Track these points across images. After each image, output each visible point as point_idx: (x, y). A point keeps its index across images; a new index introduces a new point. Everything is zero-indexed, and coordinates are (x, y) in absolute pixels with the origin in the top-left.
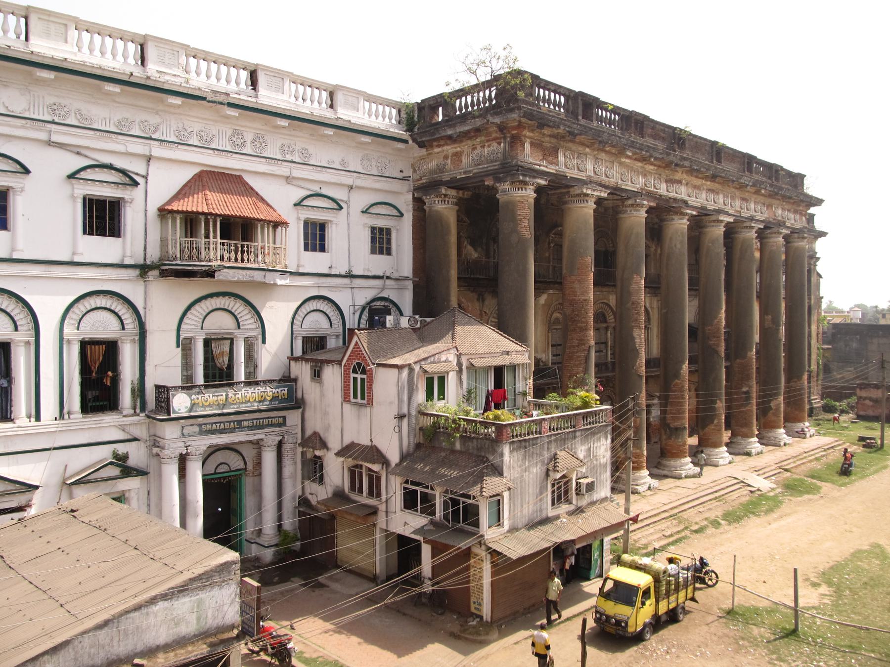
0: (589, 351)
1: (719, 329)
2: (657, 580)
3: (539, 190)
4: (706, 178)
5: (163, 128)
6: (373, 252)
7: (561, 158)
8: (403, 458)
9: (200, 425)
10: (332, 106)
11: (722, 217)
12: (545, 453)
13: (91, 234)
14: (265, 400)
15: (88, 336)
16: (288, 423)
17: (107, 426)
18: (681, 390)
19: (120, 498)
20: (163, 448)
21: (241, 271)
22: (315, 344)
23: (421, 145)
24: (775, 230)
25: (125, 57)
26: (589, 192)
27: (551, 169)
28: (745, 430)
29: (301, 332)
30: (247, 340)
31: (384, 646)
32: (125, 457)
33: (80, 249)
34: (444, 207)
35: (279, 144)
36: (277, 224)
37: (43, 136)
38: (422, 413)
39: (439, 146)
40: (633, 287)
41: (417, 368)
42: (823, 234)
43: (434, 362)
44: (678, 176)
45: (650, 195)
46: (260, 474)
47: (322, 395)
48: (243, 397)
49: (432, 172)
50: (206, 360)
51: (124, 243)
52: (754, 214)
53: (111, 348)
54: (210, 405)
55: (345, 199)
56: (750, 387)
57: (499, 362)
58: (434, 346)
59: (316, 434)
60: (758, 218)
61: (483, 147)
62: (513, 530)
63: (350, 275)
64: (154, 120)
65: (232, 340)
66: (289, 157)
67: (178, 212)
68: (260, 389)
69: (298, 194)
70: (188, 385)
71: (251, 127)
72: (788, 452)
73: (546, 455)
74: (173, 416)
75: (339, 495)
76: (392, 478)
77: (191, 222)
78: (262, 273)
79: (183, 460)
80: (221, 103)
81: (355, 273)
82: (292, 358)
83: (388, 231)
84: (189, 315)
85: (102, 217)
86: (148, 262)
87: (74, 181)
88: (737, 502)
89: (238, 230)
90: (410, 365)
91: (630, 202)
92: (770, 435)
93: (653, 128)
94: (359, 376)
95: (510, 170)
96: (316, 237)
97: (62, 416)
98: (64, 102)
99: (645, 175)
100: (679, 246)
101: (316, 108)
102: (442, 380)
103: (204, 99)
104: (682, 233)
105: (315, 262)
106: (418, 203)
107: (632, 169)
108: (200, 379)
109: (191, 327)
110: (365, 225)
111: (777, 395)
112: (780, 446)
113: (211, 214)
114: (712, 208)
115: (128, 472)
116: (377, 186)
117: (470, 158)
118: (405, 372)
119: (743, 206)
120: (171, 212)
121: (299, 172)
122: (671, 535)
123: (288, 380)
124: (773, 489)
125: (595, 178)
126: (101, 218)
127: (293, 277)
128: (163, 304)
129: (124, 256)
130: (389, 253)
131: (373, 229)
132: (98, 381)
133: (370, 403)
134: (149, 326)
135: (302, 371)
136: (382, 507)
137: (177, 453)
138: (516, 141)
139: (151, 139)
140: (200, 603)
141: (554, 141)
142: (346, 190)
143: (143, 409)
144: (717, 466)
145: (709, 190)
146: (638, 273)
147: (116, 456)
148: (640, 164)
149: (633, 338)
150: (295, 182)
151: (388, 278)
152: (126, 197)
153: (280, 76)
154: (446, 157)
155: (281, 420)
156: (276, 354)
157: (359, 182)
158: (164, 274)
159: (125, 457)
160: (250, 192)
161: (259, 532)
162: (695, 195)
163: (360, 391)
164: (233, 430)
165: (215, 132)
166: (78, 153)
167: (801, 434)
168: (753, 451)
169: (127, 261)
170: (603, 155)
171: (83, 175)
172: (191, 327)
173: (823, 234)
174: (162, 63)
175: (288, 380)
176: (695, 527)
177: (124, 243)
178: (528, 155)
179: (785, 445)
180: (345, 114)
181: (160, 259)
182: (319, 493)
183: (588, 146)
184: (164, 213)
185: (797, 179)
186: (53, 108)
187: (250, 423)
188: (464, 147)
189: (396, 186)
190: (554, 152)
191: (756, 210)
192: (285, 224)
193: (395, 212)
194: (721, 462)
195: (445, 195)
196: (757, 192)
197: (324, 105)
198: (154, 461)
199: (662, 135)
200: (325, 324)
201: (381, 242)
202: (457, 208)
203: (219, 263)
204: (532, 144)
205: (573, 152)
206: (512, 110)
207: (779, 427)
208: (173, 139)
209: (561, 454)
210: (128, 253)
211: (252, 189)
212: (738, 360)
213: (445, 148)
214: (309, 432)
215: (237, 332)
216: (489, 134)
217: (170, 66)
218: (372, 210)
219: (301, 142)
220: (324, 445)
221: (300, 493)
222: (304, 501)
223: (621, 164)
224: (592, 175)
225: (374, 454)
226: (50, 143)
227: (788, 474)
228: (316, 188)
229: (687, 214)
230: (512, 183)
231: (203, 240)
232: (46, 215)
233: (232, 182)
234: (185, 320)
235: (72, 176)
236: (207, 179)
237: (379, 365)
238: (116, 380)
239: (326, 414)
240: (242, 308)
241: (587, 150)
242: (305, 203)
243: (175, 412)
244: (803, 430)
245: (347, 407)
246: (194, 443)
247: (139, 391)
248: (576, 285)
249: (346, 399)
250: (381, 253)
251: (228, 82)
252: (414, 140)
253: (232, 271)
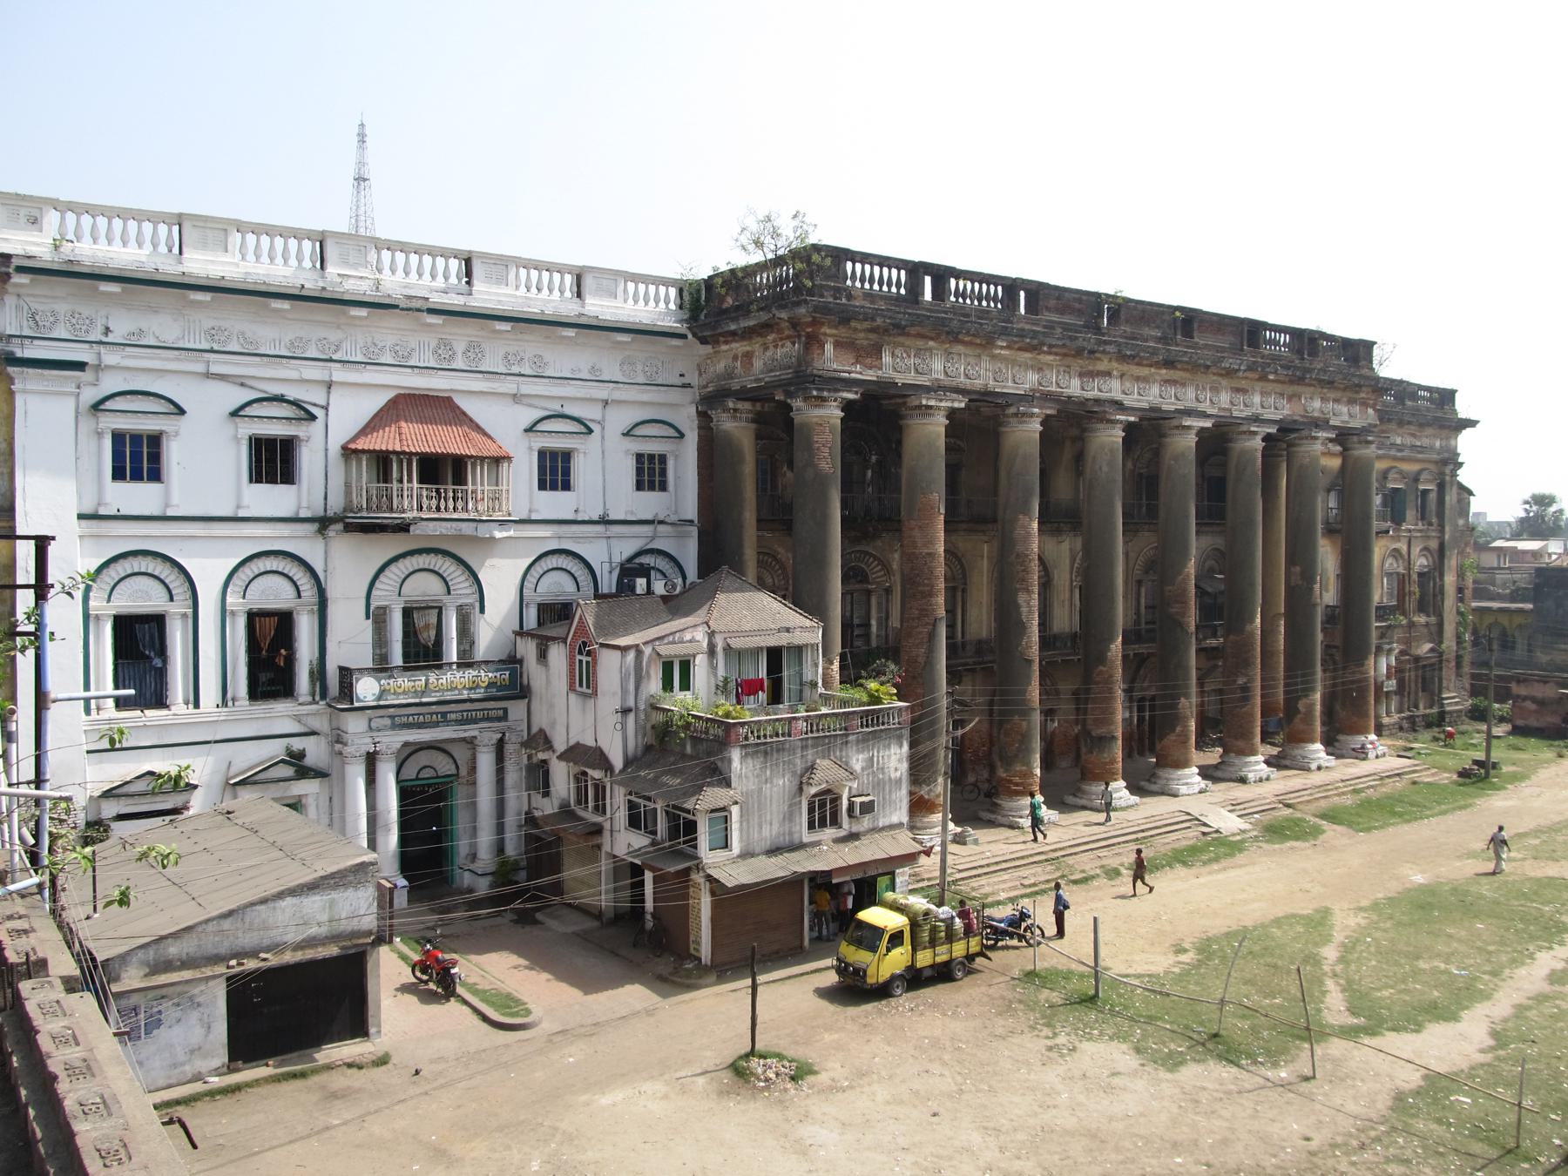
0: (934, 625)
1: (1185, 591)
2: (914, 925)
3: (847, 406)
4: (1157, 365)
5: (346, 345)
6: (639, 486)
7: (887, 359)
8: (628, 763)
9: (392, 717)
10: (579, 295)
11: (1187, 422)
12: (798, 761)
13: (259, 481)
14: (478, 686)
15: (256, 607)
16: (511, 716)
17: (279, 716)
18: (1109, 680)
19: (296, 805)
20: (345, 744)
21: (444, 524)
22: (556, 613)
23: (704, 341)
24: (1305, 433)
25: (300, 260)
26: (932, 403)
27: (870, 375)
28: (1241, 744)
29: (536, 596)
30: (460, 608)
31: (572, 985)
32: (301, 755)
33: (246, 501)
34: (736, 426)
35: (502, 353)
36: (497, 461)
37: (200, 368)
38: (655, 708)
39: (726, 342)
40: (1019, 532)
41: (647, 650)
42: (1471, 423)
43: (673, 642)
44: (1103, 366)
45: (1048, 397)
46: (474, 783)
47: (548, 681)
48: (451, 681)
49: (719, 377)
50: (406, 634)
51: (299, 490)
52: (1260, 411)
53: (285, 621)
54: (404, 693)
55: (598, 417)
56: (1251, 680)
57: (772, 641)
58: (683, 620)
59: (541, 731)
60: (1266, 417)
61: (776, 347)
62: (746, 855)
63: (604, 521)
64: (334, 336)
65: (440, 609)
66: (515, 369)
67: (363, 451)
68: (472, 673)
69: (529, 415)
70: (381, 667)
71: (461, 336)
72: (1316, 778)
73: (799, 765)
74: (356, 704)
75: (566, 812)
76: (616, 787)
77: (383, 463)
78: (473, 525)
79: (371, 760)
80: (418, 310)
81: (612, 517)
82: (521, 633)
83: (663, 459)
84: (382, 578)
85: (272, 461)
86: (330, 513)
87: (238, 420)
88: (1169, 847)
89: (441, 471)
90: (637, 646)
91: (1012, 410)
92: (1296, 752)
93: (1058, 299)
94: (585, 659)
95: (805, 381)
96: (555, 471)
97: (225, 703)
98: (224, 324)
99: (1040, 370)
100: (1105, 469)
101: (553, 300)
102: (686, 666)
103: (396, 307)
104: (1111, 451)
105: (556, 504)
106: (703, 416)
107: (1014, 362)
108: (397, 658)
109: (381, 596)
110: (627, 452)
111: (1313, 689)
112: (1309, 770)
113: (404, 453)
114: (1172, 408)
115: (304, 772)
116: (645, 397)
117: (763, 360)
118: (631, 655)
119: (1236, 401)
120: (356, 451)
121: (529, 387)
122: (1034, 885)
123: (512, 662)
124: (1244, 831)
125: (947, 382)
126: (271, 461)
127: (520, 527)
128: (349, 567)
129: (299, 507)
130: (663, 487)
131: (639, 457)
132: (270, 660)
133: (595, 693)
134: (330, 594)
135: (528, 649)
136: (607, 826)
137: (364, 749)
138: (813, 342)
139: (331, 360)
140: (332, 903)
141: (872, 336)
142: (600, 406)
143: (323, 697)
144: (1175, 796)
145: (1166, 381)
146: (1026, 511)
147: (291, 753)
148: (1028, 355)
149: (1018, 607)
150: (525, 400)
151: (661, 522)
152: (301, 434)
153: (503, 264)
154: (735, 358)
155: (501, 713)
156: (499, 629)
157: (617, 395)
158: (350, 528)
159: (301, 755)
160: (459, 417)
161: (473, 857)
162: (1135, 391)
163: (584, 680)
164: (436, 725)
165: (414, 344)
166: (242, 385)
167: (1361, 754)
168: (1251, 776)
169: (302, 515)
170: (960, 348)
171: (248, 411)
172: (385, 593)
173: (1471, 423)
174: (345, 262)
175: (512, 662)
176: (1077, 876)
177: (299, 490)
178: (831, 359)
179: (1319, 768)
180: (598, 306)
181: (345, 510)
182: (546, 808)
183: (932, 339)
184: (348, 452)
185: (1358, 352)
186: (211, 334)
187: (459, 716)
188: (755, 346)
189: (675, 396)
190: (876, 351)
191: (1264, 406)
192: (508, 458)
193: (672, 432)
194: (1183, 790)
195: (735, 410)
196: (1263, 378)
197: (568, 294)
198: (337, 761)
199: (1077, 305)
200: (570, 587)
201: (651, 473)
202: (753, 426)
203: (415, 514)
204: (837, 345)
205: (907, 349)
206: (798, 304)
207: (1313, 741)
208: (360, 358)
209: (822, 763)
210: (304, 504)
211: (464, 414)
212: (1232, 637)
213: (734, 345)
214: (534, 730)
215: (446, 599)
216: (780, 331)
217: (355, 266)
218: (637, 432)
219: (531, 346)
220: (548, 744)
221: (526, 808)
222: (530, 820)
223: (994, 357)
224: (942, 377)
225: (598, 757)
226: (208, 375)
227: (1289, 811)
228: (555, 407)
229: (1118, 421)
230: (806, 399)
231: (395, 485)
232: (207, 464)
233: (440, 408)
234: (378, 585)
235: (235, 414)
236: (405, 406)
237: (602, 645)
238: (291, 660)
239: (552, 706)
240: (452, 568)
241: (931, 343)
242: (540, 427)
243: (359, 700)
244: (1363, 747)
245: (572, 696)
246: (384, 740)
247: (319, 674)
248: (916, 533)
249: (571, 688)
250: (652, 488)
251: (433, 277)
252: (694, 335)
253: (431, 524)
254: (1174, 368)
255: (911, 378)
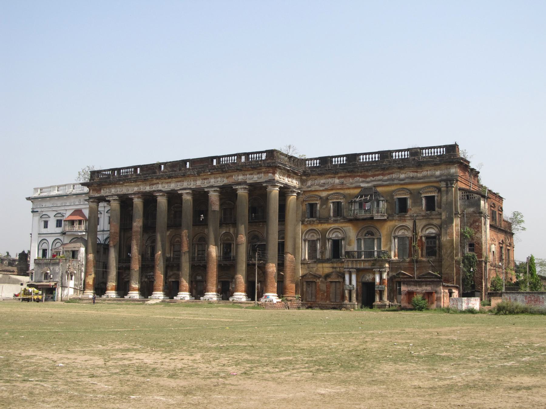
7: (102, 191)
45: (139, 193)
64: (66, 201)
85: (59, 223)
107: (131, 186)
170: (117, 186)
190: (100, 190)
205: (106, 188)
254: (177, 178)
255: (107, 194)
